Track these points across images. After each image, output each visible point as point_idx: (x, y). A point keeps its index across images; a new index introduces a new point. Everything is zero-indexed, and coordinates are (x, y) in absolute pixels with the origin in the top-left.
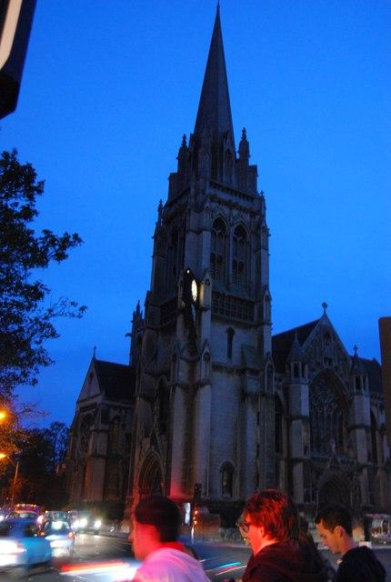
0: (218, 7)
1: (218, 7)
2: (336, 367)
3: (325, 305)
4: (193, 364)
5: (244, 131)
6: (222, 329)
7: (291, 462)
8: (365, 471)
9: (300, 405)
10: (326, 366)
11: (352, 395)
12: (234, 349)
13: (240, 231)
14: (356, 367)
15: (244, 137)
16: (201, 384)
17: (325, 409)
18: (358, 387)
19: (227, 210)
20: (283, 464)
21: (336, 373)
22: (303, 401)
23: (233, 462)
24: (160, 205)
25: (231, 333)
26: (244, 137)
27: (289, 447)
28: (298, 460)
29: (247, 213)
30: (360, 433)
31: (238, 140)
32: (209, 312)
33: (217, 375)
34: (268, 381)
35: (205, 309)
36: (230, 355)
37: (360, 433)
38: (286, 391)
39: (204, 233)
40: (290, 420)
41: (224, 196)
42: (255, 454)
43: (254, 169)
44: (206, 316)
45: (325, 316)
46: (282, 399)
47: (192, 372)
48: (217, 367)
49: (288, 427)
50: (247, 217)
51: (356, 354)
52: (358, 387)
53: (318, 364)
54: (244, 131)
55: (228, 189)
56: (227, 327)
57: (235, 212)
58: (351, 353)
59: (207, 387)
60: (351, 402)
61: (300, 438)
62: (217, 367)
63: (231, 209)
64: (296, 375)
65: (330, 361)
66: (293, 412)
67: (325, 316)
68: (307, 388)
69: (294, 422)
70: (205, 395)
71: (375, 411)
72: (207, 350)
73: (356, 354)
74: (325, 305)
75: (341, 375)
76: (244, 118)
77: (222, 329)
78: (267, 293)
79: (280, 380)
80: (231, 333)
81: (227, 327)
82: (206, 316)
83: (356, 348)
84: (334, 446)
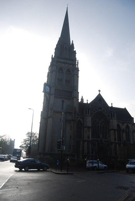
0: (67, 8)
1: (67, 8)
2: (103, 111)
3: (99, 91)
5: (73, 41)
8: (113, 144)
10: (100, 110)
13: (68, 70)
14: (111, 110)
15: (72, 42)
17: (99, 124)
18: (112, 116)
20: (81, 143)
22: (89, 121)
26: (72, 42)
28: (86, 141)
29: (71, 65)
30: (112, 132)
32: (53, 95)
36: (62, 108)
37: (112, 132)
41: (63, 61)
43: (75, 52)
45: (99, 95)
50: (71, 66)
51: (112, 106)
52: (112, 116)
54: (73, 41)
55: (64, 58)
56: (62, 100)
57: (67, 65)
58: (110, 105)
59: (51, 119)
60: (109, 121)
61: (88, 134)
63: (65, 64)
64: (86, 114)
65: (101, 109)
67: (99, 95)
68: (90, 118)
71: (120, 124)
72: (52, 107)
73: (112, 106)
74: (99, 91)
76: (73, 38)
78: (75, 88)
79: (81, 116)
80: (63, 101)
83: (112, 104)
84: (101, 136)
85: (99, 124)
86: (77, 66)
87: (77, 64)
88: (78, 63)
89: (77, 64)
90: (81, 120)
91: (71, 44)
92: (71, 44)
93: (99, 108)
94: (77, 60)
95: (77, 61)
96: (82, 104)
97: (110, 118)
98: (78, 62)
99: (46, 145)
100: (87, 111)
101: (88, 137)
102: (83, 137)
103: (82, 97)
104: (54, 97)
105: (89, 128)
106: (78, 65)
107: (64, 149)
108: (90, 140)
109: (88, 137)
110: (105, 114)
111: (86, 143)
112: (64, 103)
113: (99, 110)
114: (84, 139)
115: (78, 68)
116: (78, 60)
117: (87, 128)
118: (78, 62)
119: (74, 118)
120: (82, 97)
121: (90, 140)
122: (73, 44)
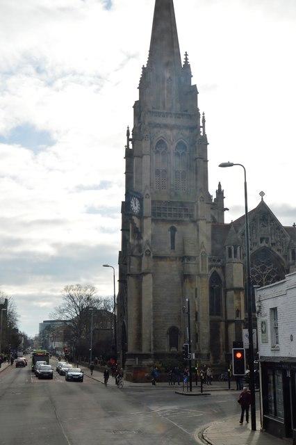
3: (262, 194)
4: (140, 258)
5: (186, 55)
6: (165, 229)
7: (228, 323)
9: (232, 279)
11: (289, 265)
12: (176, 242)
15: (186, 59)
16: (145, 274)
17: (264, 279)
19: (169, 132)
21: (274, 249)
23: (178, 327)
24: (128, 131)
25: (173, 230)
26: (186, 59)
27: (226, 315)
28: (233, 321)
31: (183, 60)
32: (149, 219)
33: (162, 263)
34: (202, 264)
35: (146, 217)
36: (173, 247)
38: (223, 267)
39: (144, 156)
40: (226, 291)
42: (194, 319)
44: (148, 223)
45: (262, 204)
46: (222, 278)
47: (140, 264)
48: (162, 258)
49: (226, 297)
50: (187, 133)
53: (255, 244)
54: (186, 55)
56: (170, 226)
59: (150, 276)
62: (162, 258)
63: (171, 130)
64: (230, 256)
65: (268, 239)
66: (228, 286)
67: (262, 204)
68: (241, 266)
69: (229, 293)
70: (148, 281)
75: (278, 250)
77: (165, 229)
81: (169, 226)
82: (148, 223)
85: (264, 279)
86: (201, 129)
87: (201, 125)
88: (204, 121)
89: (201, 125)
90: (219, 271)
91: (183, 63)
92: (183, 63)
93: (262, 240)
94: (201, 113)
95: (201, 116)
96: (219, 228)
97: (291, 261)
98: (204, 117)
99: (143, 336)
100: (233, 250)
101: (238, 312)
102: (226, 311)
103: (220, 186)
104: (153, 220)
105: (238, 290)
106: (204, 127)
107: (194, 357)
108: (243, 318)
109: (238, 312)
110: (277, 252)
111: (232, 327)
112: (176, 233)
113: (263, 245)
114: (226, 318)
115: (205, 135)
116: (203, 114)
117: (233, 292)
118: (204, 117)
119: (202, 270)
120: (220, 186)
121: (243, 318)
122: (187, 66)
